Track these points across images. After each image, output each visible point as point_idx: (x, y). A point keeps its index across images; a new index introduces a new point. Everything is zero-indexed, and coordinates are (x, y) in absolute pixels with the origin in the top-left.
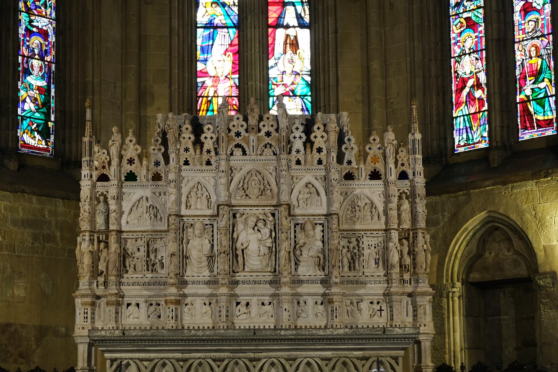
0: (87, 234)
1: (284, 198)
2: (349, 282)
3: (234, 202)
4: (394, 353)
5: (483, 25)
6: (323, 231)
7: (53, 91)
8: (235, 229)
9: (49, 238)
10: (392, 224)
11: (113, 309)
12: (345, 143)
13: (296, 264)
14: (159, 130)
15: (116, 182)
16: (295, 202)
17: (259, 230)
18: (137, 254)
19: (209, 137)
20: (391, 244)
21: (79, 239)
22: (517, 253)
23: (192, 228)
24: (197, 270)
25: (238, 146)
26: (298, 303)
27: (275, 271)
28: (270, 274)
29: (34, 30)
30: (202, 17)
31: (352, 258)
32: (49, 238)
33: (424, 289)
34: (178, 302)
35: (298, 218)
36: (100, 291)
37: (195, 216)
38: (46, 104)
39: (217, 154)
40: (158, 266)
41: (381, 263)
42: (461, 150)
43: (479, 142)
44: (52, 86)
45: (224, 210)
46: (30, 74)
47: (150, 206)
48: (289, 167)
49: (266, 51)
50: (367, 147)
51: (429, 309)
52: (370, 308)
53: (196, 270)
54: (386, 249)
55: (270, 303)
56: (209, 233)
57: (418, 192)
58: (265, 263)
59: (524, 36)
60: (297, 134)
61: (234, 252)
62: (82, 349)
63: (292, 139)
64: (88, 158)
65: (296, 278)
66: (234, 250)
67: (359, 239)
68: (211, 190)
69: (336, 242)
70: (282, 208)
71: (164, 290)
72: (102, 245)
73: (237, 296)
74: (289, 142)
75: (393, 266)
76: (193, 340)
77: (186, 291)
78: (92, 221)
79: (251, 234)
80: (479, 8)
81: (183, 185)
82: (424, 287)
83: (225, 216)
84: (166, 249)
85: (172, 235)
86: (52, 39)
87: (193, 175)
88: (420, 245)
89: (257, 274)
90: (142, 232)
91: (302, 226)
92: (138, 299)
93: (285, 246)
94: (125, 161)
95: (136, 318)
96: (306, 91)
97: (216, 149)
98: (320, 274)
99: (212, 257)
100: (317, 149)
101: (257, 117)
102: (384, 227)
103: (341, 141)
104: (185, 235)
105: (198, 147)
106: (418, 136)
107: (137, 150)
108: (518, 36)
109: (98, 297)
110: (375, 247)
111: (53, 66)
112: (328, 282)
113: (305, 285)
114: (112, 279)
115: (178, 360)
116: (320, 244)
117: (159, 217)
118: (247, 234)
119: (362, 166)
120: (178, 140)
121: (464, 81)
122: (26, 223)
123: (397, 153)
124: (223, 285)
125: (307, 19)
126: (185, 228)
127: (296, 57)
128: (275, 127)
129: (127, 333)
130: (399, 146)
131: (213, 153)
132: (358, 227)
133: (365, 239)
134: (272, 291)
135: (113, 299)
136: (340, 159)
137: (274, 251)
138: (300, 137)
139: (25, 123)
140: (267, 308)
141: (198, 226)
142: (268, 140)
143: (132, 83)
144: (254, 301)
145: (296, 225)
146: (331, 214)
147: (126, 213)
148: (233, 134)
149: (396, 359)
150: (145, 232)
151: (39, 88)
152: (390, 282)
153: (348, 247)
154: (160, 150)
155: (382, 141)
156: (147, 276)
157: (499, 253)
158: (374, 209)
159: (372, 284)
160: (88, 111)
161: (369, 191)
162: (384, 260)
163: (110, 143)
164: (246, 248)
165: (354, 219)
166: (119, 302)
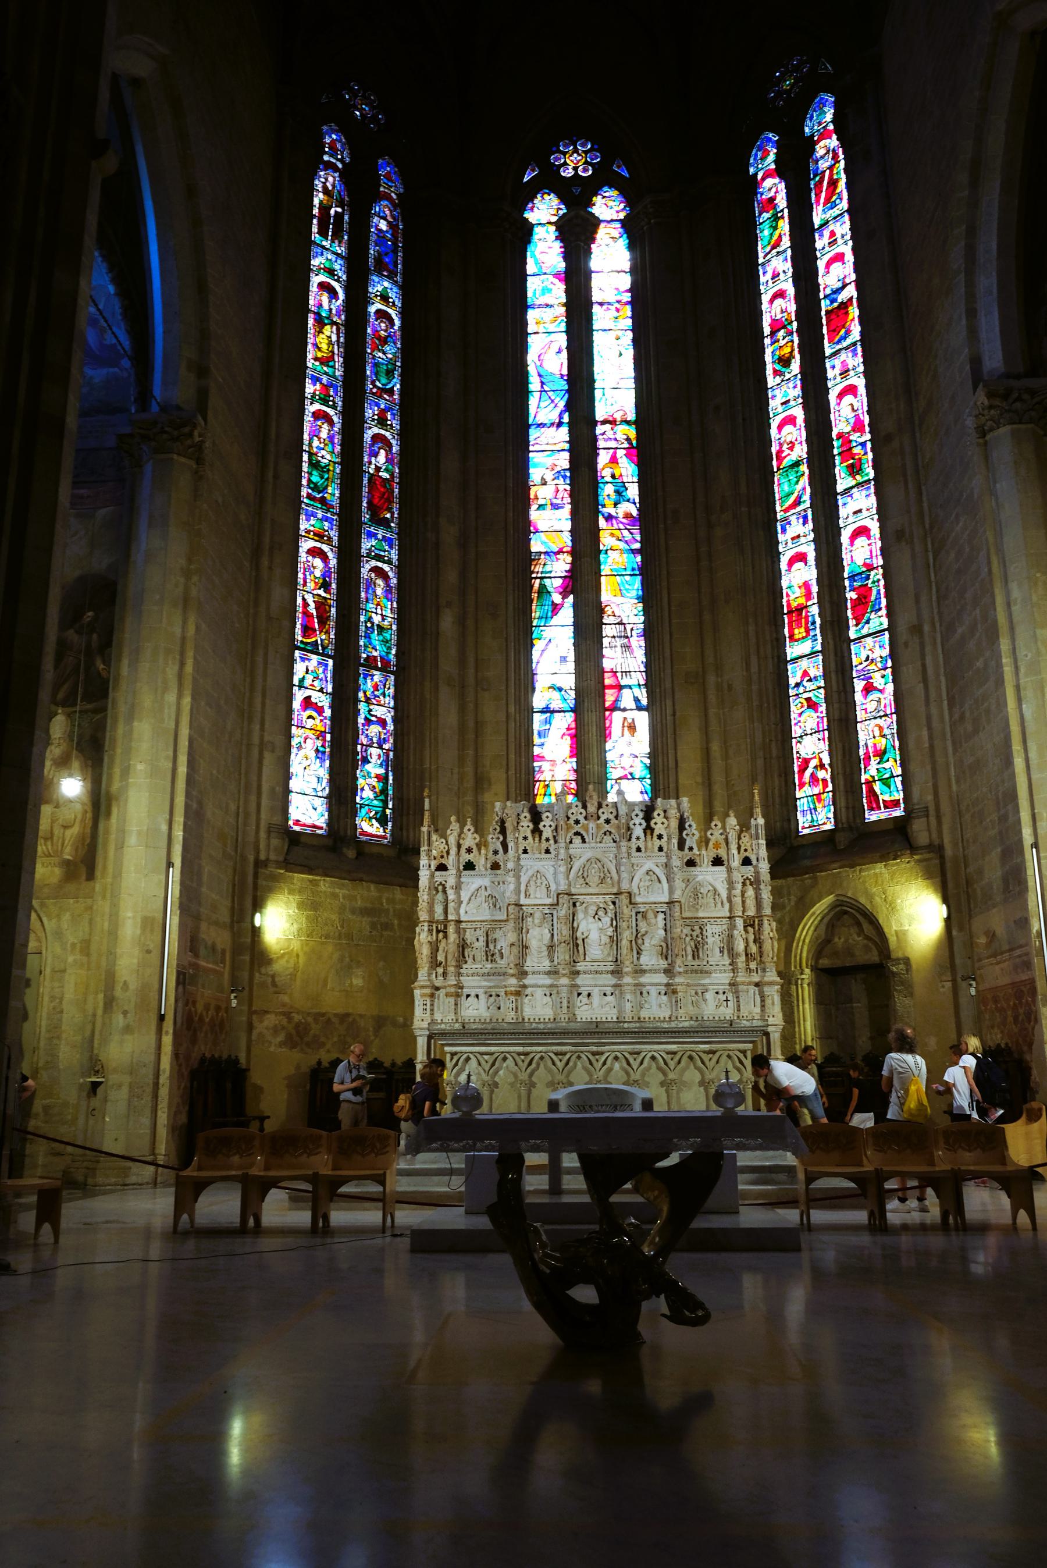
0: (426, 924)
1: (625, 886)
2: (692, 972)
3: (573, 891)
4: (741, 1046)
5: (824, 705)
7: (391, 778)
9: (387, 926)
11: (452, 1000)
14: (497, 819)
15: (454, 872)
16: (635, 890)
18: (476, 944)
19: (548, 825)
20: (736, 932)
21: (418, 929)
22: (867, 938)
24: (537, 961)
25: (577, 834)
26: (641, 993)
29: (374, 719)
30: (538, 701)
31: (696, 947)
32: (387, 926)
33: (771, 979)
34: (518, 994)
36: (439, 982)
38: (384, 791)
39: (556, 842)
40: (497, 957)
42: (806, 831)
43: (824, 824)
44: (390, 774)
46: (369, 762)
48: (629, 854)
49: (604, 734)
50: (709, 833)
51: (777, 999)
53: (535, 960)
54: (731, 937)
57: (762, 878)
58: (606, 953)
60: (637, 821)
62: (421, 1042)
63: (632, 826)
64: (426, 848)
68: (551, 878)
69: (679, 930)
70: (623, 897)
71: (504, 981)
72: (441, 935)
73: (578, 986)
74: (629, 829)
75: (738, 955)
76: (534, 1033)
77: (526, 982)
78: (431, 911)
80: (819, 688)
81: (522, 874)
82: (772, 976)
84: (506, 938)
85: (511, 925)
86: (390, 727)
87: (531, 864)
88: (766, 933)
93: (627, 935)
94: (463, 850)
95: (475, 1010)
96: (646, 773)
97: (554, 837)
98: (663, 964)
101: (596, 804)
102: (728, 915)
103: (681, 827)
106: (761, 821)
108: (860, 715)
109: (437, 989)
111: (391, 754)
114: (451, 969)
115: (519, 1054)
116: (663, 932)
119: (704, 852)
120: (516, 829)
121: (806, 762)
122: (365, 912)
123: (739, 838)
125: (644, 702)
128: (615, 814)
129: (467, 1026)
130: (741, 831)
131: (552, 842)
132: (701, 915)
133: (708, 927)
134: (614, 981)
135: (453, 990)
136: (681, 846)
137: (615, 940)
138: (640, 824)
139: (364, 811)
142: (607, 827)
143: (469, 769)
144: (596, 992)
145: (637, 913)
148: (571, 822)
149: (744, 1052)
151: (378, 776)
154: (498, 838)
155: (724, 827)
157: (848, 938)
160: (427, 801)
161: (712, 877)
162: (729, 949)
163: (449, 832)
166: (458, 994)
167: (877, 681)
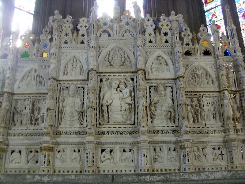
6: (172, 92)
8: (102, 90)
10: (224, 87)
12: (183, 31)
13: (151, 118)
17: (121, 91)
23: (67, 91)
27: (134, 124)
28: (130, 126)
35: (152, 81)
37: (70, 80)
41: (218, 118)
45: (93, 75)
48: (144, 45)
52: (213, 153)
55: (130, 150)
56: (81, 94)
58: (125, 117)
61: (100, 108)
65: (152, 129)
66: (100, 107)
67: (200, 99)
70: (139, 72)
79: (115, 93)
83: (93, 79)
89: (119, 126)
90: (29, 94)
91: (156, 88)
92: (21, 147)
99: (82, 113)
100: (164, 33)
104: (61, 95)
110: (212, 105)
112: (179, 132)
113: (160, 134)
116: (171, 101)
118: (111, 94)
124: (90, 134)
126: (62, 89)
132: (198, 90)
133: (204, 99)
137: (133, 107)
140: (128, 154)
141: (72, 87)
146: (178, 78)
150: (31, 94)
152: (227, 131)
153: (191, 105)
158: (208, 77)
159: (212, 133)
164: (110, 104)
165: (195, 84)
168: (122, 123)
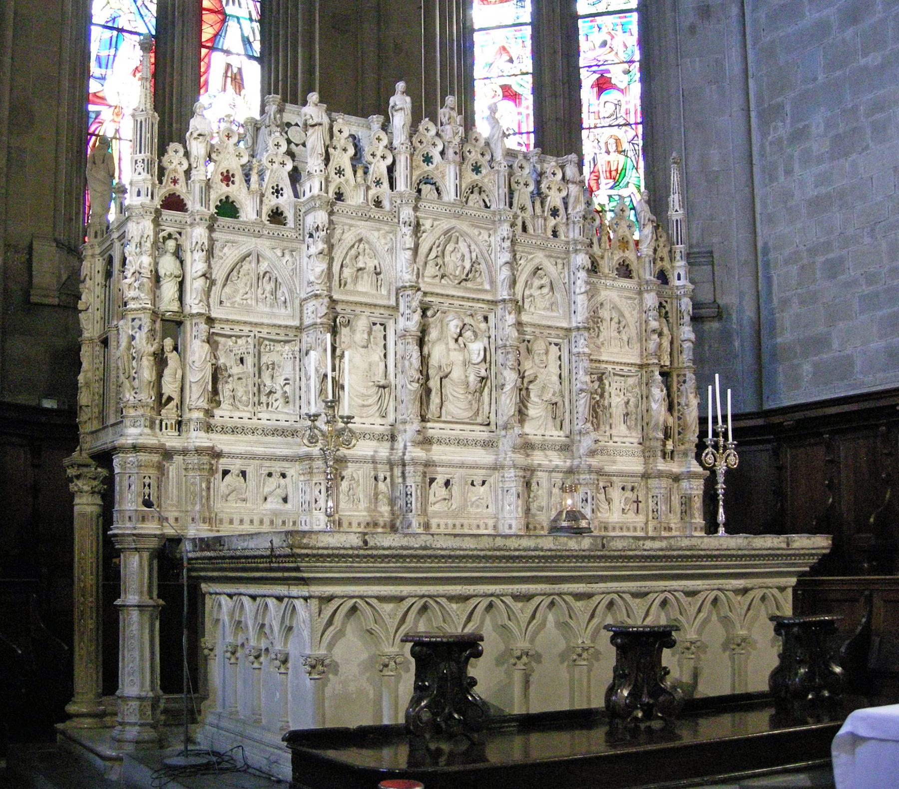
23: (348, 328)
28: (483, 428)
47: (266, 273)
59: (598, 121)
79: (455, 349)
90: (251, 323)
102: (638, 362)
105: (360, 173)
107: (239, 156)
108: (587, 120)
117: (283, 299)
125: (257, 46)
127: (239, 100)
147: (219, 283)
156: (260, 415)
167: (616, 75)
168: (468, 421)
